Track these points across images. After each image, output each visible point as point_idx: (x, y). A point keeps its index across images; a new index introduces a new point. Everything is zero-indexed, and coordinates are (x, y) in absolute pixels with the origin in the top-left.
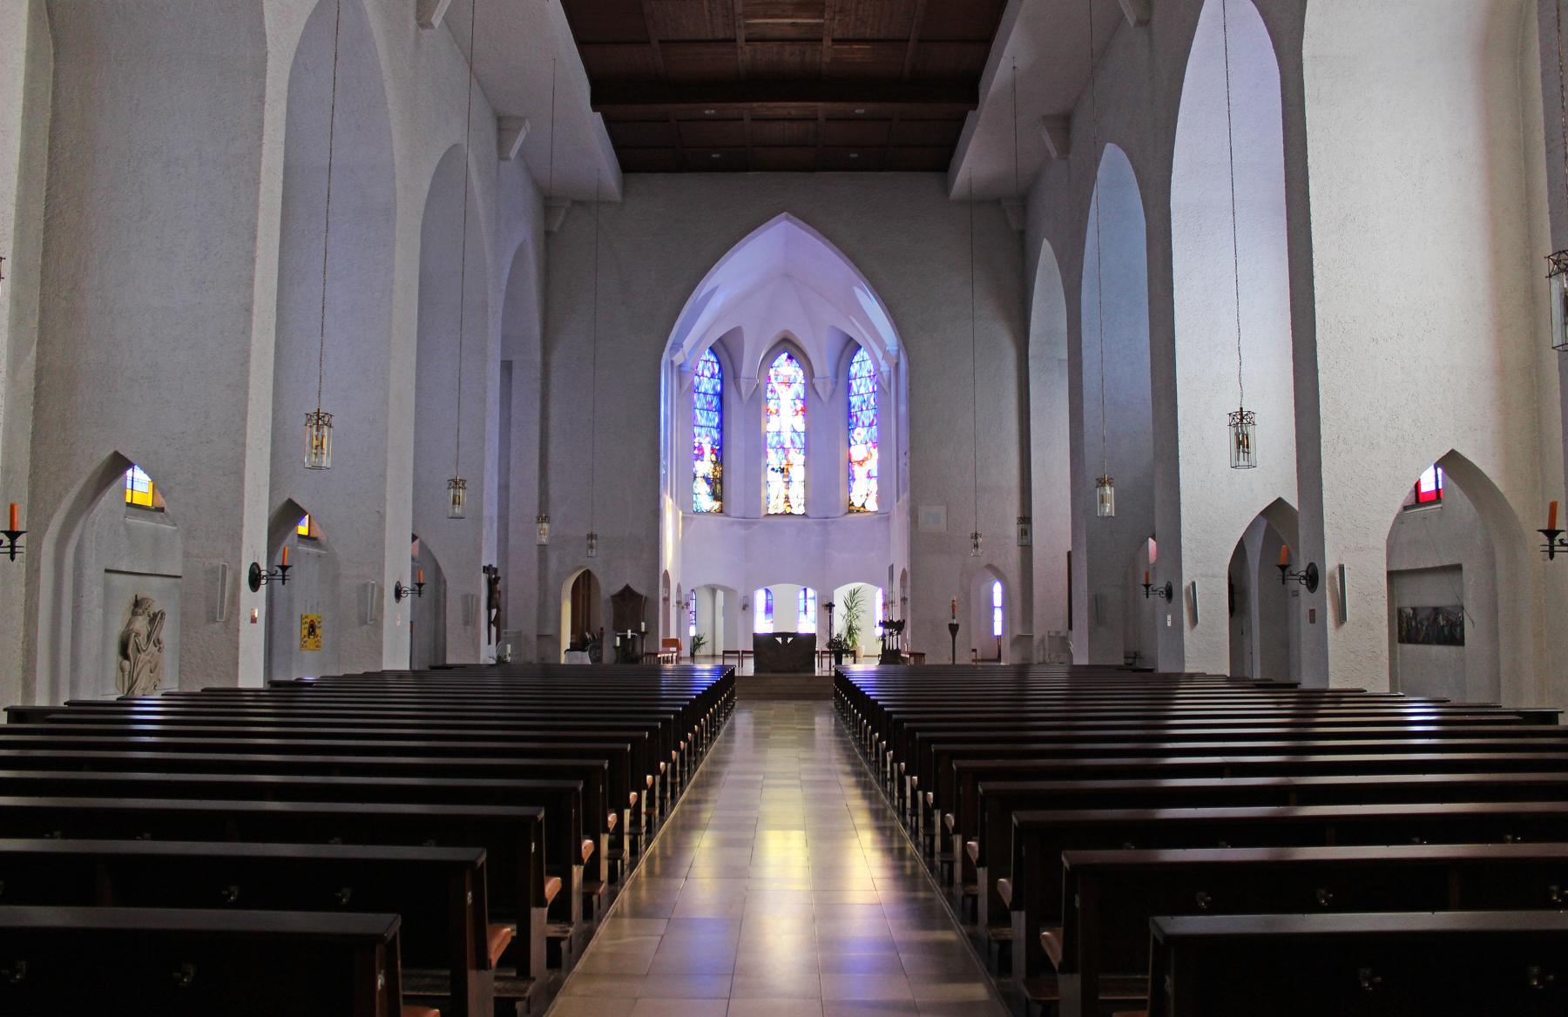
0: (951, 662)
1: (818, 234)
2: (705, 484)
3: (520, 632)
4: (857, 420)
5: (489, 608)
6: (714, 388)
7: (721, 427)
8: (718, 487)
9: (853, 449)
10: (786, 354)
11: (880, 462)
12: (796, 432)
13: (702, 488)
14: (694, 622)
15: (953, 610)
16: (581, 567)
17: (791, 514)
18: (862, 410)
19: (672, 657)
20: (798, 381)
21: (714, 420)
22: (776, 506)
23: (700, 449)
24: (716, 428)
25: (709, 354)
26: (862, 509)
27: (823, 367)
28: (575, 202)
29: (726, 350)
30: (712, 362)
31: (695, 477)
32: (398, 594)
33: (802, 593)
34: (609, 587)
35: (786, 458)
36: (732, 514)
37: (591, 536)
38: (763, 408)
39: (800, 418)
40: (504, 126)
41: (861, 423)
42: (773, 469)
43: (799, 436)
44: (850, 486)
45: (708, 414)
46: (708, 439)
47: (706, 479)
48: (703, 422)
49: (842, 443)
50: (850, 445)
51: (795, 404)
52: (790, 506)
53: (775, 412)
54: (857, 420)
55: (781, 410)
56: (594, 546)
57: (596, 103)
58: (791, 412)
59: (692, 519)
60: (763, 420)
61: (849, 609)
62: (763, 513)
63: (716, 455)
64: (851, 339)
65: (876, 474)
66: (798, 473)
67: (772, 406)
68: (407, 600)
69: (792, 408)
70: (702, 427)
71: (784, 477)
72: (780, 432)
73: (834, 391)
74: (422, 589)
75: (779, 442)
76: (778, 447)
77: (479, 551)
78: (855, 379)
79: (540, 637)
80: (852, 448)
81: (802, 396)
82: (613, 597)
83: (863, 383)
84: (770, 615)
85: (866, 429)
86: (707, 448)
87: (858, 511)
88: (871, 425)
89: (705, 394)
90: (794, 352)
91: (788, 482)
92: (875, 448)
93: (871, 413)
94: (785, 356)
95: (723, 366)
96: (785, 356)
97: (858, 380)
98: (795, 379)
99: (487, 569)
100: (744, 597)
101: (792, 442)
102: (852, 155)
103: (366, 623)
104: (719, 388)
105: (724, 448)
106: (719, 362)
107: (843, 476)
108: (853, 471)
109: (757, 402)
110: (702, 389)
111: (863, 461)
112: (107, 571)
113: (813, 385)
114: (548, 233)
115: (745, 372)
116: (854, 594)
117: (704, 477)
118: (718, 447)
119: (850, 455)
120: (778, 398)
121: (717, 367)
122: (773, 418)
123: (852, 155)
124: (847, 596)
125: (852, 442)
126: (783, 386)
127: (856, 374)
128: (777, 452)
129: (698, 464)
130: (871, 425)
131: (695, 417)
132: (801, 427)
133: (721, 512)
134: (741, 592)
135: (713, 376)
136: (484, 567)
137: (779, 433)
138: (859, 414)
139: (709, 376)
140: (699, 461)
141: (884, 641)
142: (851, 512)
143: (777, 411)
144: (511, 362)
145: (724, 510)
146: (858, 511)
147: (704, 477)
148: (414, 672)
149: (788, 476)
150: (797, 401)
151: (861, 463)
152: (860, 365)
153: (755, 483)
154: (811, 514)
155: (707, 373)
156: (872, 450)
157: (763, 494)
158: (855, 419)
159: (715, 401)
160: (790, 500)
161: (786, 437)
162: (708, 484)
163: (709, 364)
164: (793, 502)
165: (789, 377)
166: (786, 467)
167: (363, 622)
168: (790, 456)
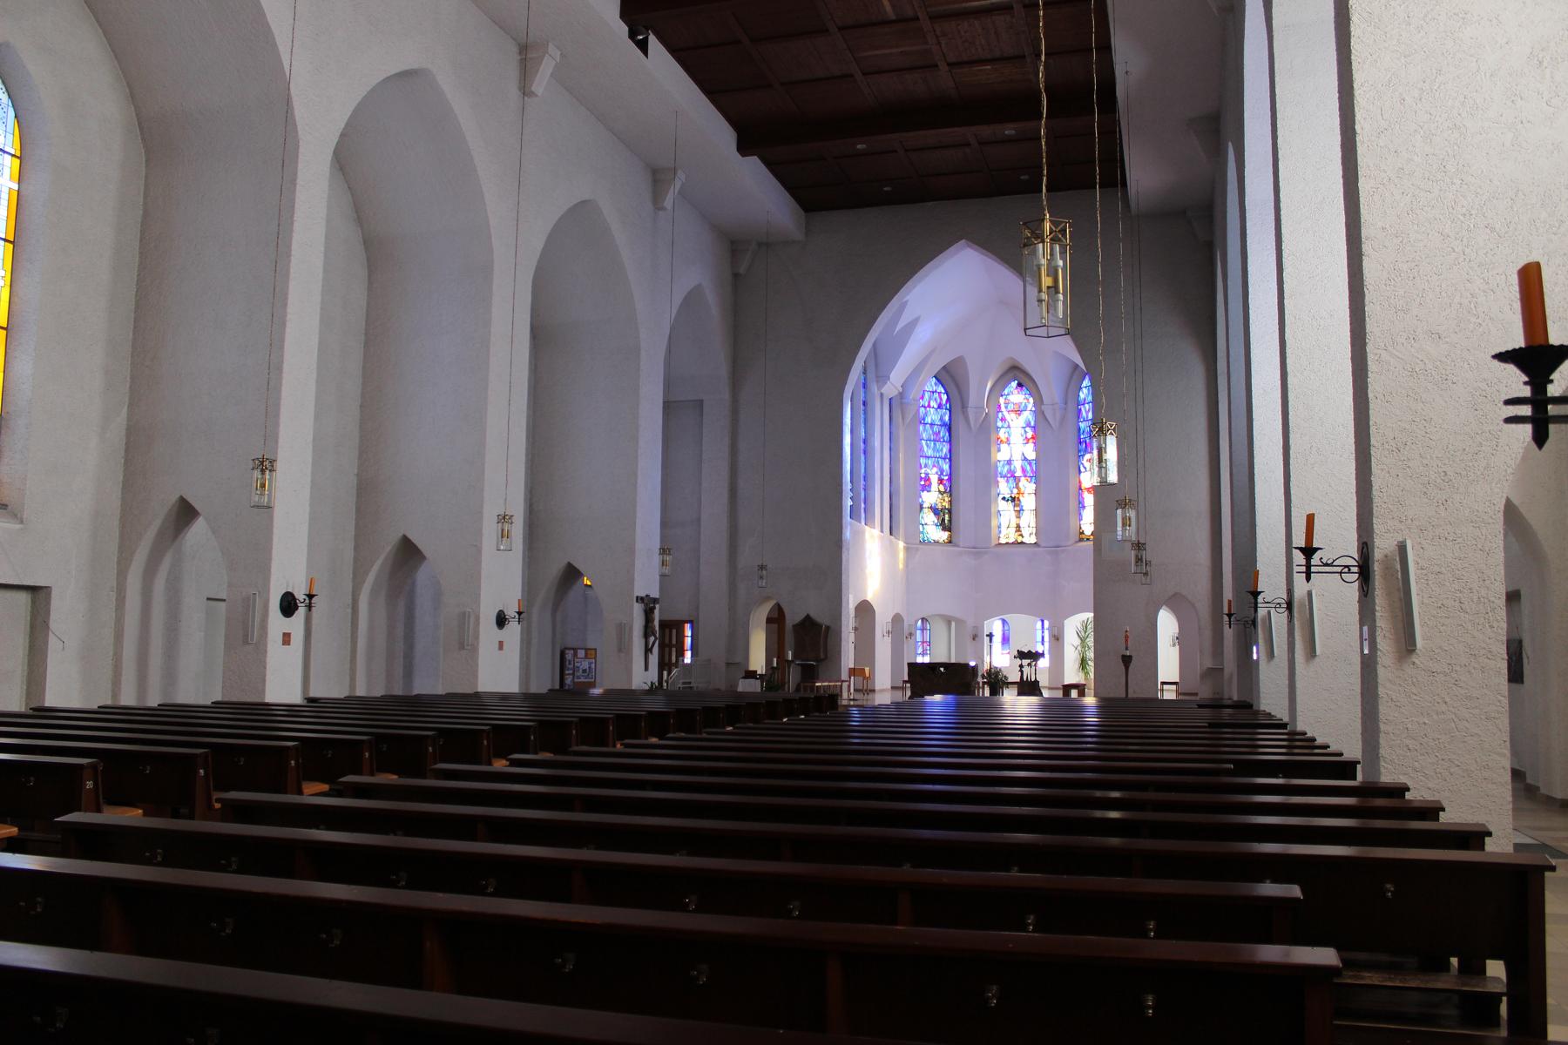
0: (1124, 696)
1: (999, 260)
2: (932, 514)
3: (710, 660)
5: (646, 636)
6: (941, 419)
7: (950, 458)
8: (946, 519)
10: (1016, 382)
12: (1027, 460)
13: (929, 518)
15: (1126, 641)
16: (768, 598)
17: (1022, 543)
19: (841, 686)
20: (1029, 409)
21: (942, 450)
22: (1008, 536)
23: (927, 479)
24: (944, 459)
27: (1052, 390)
28: (760, 244)
29: (953, 378)
30: (940, 393)
31: (921, 507)
32: (501, 621)
33: (1039, 624)
34: (793, 617)
35: (1017, 487)
36: (961, 544)
37: (762, 567)
38: (993, 437)
39: (1031, 446)
40: (658, 178)
42: (1004, 498)
43: (1030, 464)
44: (1080, 514)
45: (935, 444)
46: (935, 470)
47: (935, 511)
48: (930, 453)
49: (1072, 471)
50: (1080, 472)
52: (1021, 535)
53: (1005, 440)
55: (1011, 438)
56: (764, 577)
57: (744, 148)
58: (1021, 440)
59: (917, 549)
60: (993, 449)
62: (994, 542)
63: (944, 485)
64: (1077, 365)
66: (1029, 502)
67: (1002, 434)
68: (514, 629)
69: (1022, 435)
70: (929, 457)
72: (1010, 460)
73: (1063, 419)
74: (522, 616)
77: (631, 581)
78: (1084, 404)
79: (728, 664)
80: (1082, 474)
81: (1032, 424)
82: (794, 626)
84: (1006, 645)
86: (934, 479)
87: (1088, 539)
89: (932, 425)
90: (1025, 380)
94: (1014, 384)
95: (951, 397)
97: (1087, 406)
98: (1026, 406)
99: (640, 599)
100: (974, 627)
101: (1024, 470)
102: (1022, 177)
103: (463, 648)
104: (947, 418)
105: (953, 477)
106: (946, 393)
107: (1073, 504)
108: (1083, 498)
109: (986, 433)
110: (928, 420)
112: (208, 599)
113: (1043, 413)
114: (736, 276)
115: (972, 401)
117: (931, 508)
118: (946, 478)
119: (1080, 482)
120: (1009, 427)
121: (944, 397)
122: (1004, 447)
123: (1022, 177)
124: (1079, 626)
126: (1013, 415)
127: (1085, 399)
128: (1008, 481)
129: (925, 495)
131: (921, 449)
132: (1032, 455)
133: (950, 542)
134: (970, 622)
135: (940, 406)
136: (637, 597)
137: (1009, 462)
139: (936, 406)
140: (925, 492)
141: (1022, 672)
142: (1081, 540)
143: (1008, 439)
144: (702, 401)
145: (953, 540)
146: (1088, 539)
147: (931, 508)
148: (527, 697)
149: (1019, 505)
150: (1028, 429)
153: (985, 512)
154: (1043, 544)
155: (933, 404)
157: (994, 523)
159: (944, 433)
160: (1022, 529)
161: (1017, 465)
162: (935, 514)
163: (936, 395)
164: (1025, 532)
166: (1017, 496)
167: (462, 646)
168: (1021, 485)
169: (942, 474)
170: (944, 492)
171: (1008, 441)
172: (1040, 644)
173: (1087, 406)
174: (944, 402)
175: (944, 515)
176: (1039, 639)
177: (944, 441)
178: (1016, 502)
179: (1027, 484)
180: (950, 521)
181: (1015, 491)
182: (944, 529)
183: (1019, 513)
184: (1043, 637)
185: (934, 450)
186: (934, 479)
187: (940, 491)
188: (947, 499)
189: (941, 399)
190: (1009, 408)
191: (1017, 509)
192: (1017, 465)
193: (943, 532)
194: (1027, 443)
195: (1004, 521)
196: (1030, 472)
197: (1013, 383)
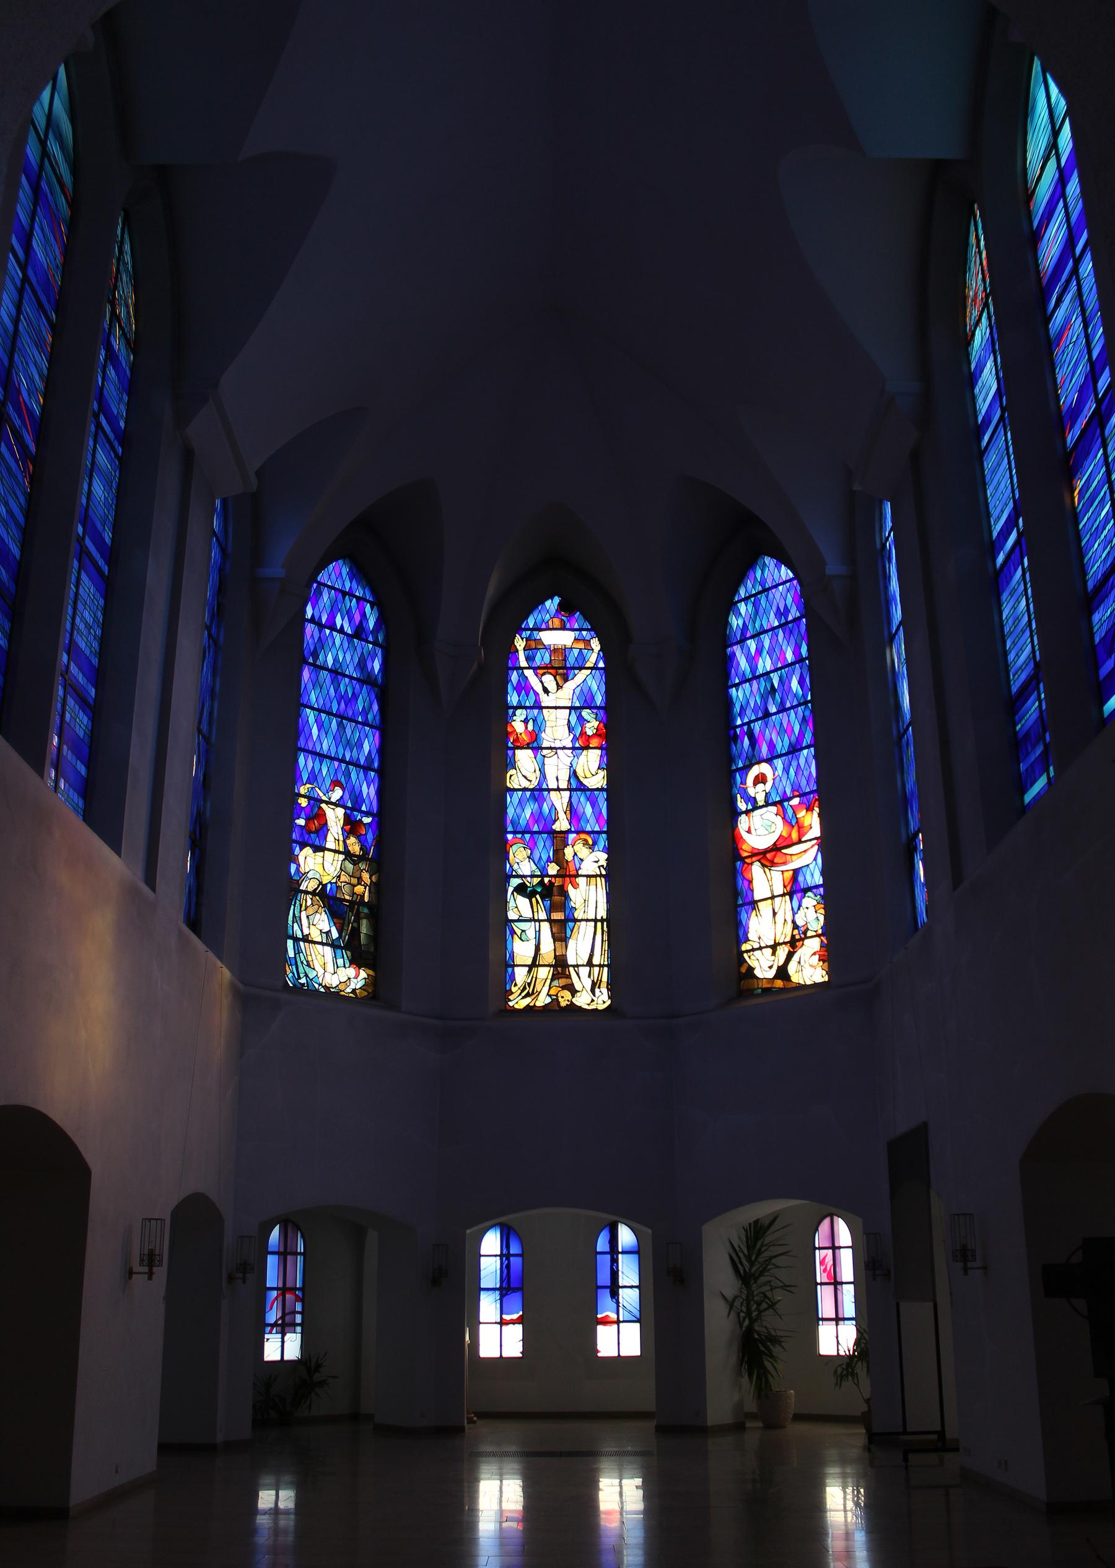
4: (754, 742)
6: (362, 665)
9: (743, 823)
10: (557, 600)
11: (824, 843)
14: (298, 1319)
17: (572, 1008)
18: (767, 715)
24: (367, 768)
25: (352, 576)
26: (779, 983)
30: (358, 599)
35: (558, 858)
41: (764, 749)
45: (340, 725)
48: (326, 745)
51: (581, 719)
54: (754, 742)
61: (745, 1279)
65: (818, 879)
69: (571, 729)
70: (322, 757)
71: (549, 912)
75: (537, 817)
76: (536, 828)
78: (743, 641)
81: (599, 700)
83: (767, 644)
85: (779, 763)
86: (335, 818)
88: (794, 749)
89: (336, 673)
91: (562, 923)
92: (810, 809)
93: (794, 720)
94: (552, 604)
96: (552, 604)
97: (752, 645)
101: (573, 813)
111: (776, 848)
116: (757, 1232)
122: (524, 757)
125: (742, 805)
130: (794, 749)
132: (597, 780)
135: (359, 633)
137: (538, 793)
138: (757, 727)
140: (308, 851)
150: (586, 713)
151: (769, 857)
152: (756, 605)
156: (801, 814)
158: (746, 741)
164: (582, 980)
165: (564, 651)
166: (558, 882)
168: (569, 852)
169: (356, 807)
170: (361, 858)
171: (534, 744)
172: (607, 1292)
173: (752, 645)
174: (371, 624)
175: (358, 920)
176: (604, 1278)
177: (365, 723)
178: (557, 898)
179: (582, 851)
180: (374, 938)
181: (553, 869)
182: (357, 961)
183: (562, 933)
184: (614, 1275)
185: (338, 739)
186: (335, 818)
187: (348, 854)
188: (366, 876)
189: (363, 615)
190: (538, 661)
191: (558, 916)
192: (560, 801)
193: (351, 972)
194: (587, 748)
195: (522, 951)
196: (593, 820)
197: (548, 603)
